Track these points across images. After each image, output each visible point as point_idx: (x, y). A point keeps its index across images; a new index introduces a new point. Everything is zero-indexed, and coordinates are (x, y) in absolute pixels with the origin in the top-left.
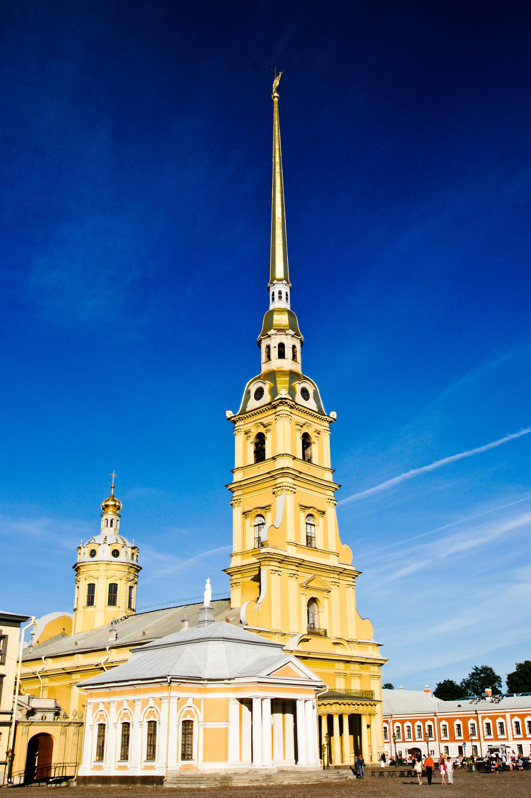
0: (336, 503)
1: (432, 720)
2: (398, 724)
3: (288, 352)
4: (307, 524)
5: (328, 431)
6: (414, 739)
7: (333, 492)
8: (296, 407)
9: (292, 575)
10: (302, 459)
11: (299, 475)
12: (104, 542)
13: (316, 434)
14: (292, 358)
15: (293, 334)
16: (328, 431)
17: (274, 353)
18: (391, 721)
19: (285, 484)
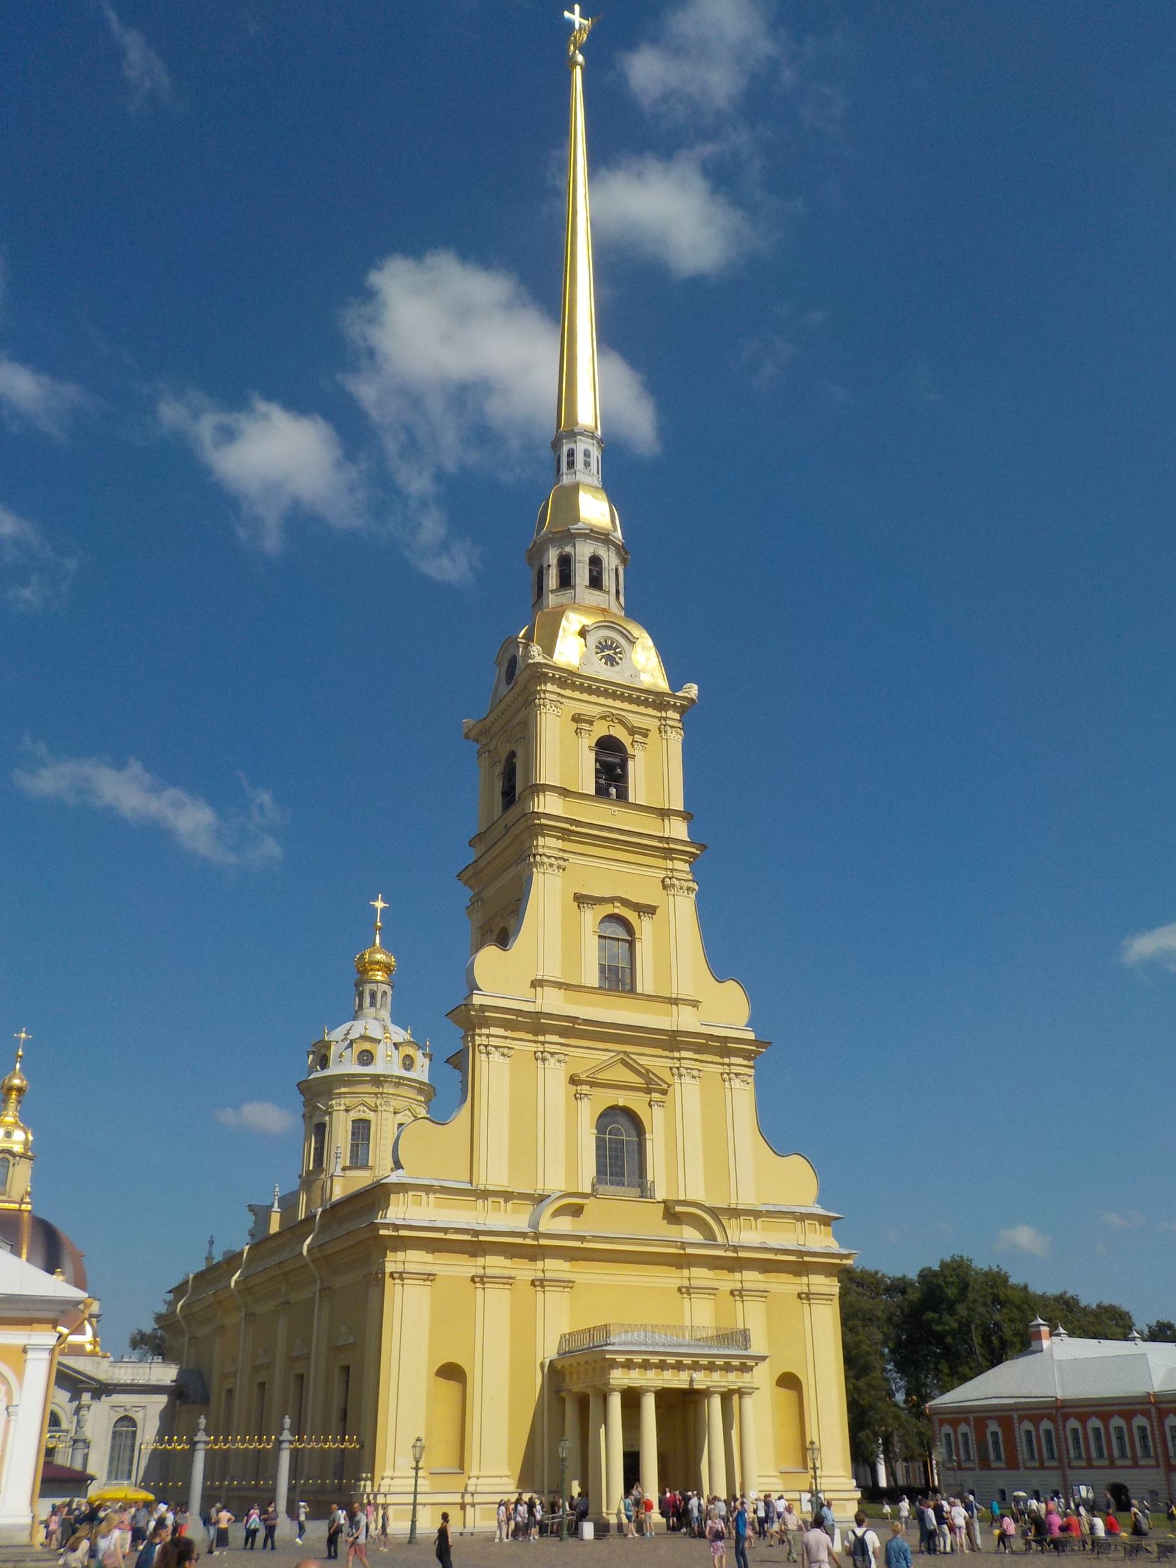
0: (696, 886)
1: (1146, 1414)
2: (1073, 1423)
3: (582, 575)
4: (600, 937)
6: (1134, 1459)
7: (685, 861)
8: (573, 683)
9: (546, 1054)
10: (594, 794)
11: (573, 828)
12: (344, 1037)
13: (638, 737)
14: (588, 584)
15: (588, 531)
17: (552, 580)
18: (1059, 1414)
19: (534, 852)
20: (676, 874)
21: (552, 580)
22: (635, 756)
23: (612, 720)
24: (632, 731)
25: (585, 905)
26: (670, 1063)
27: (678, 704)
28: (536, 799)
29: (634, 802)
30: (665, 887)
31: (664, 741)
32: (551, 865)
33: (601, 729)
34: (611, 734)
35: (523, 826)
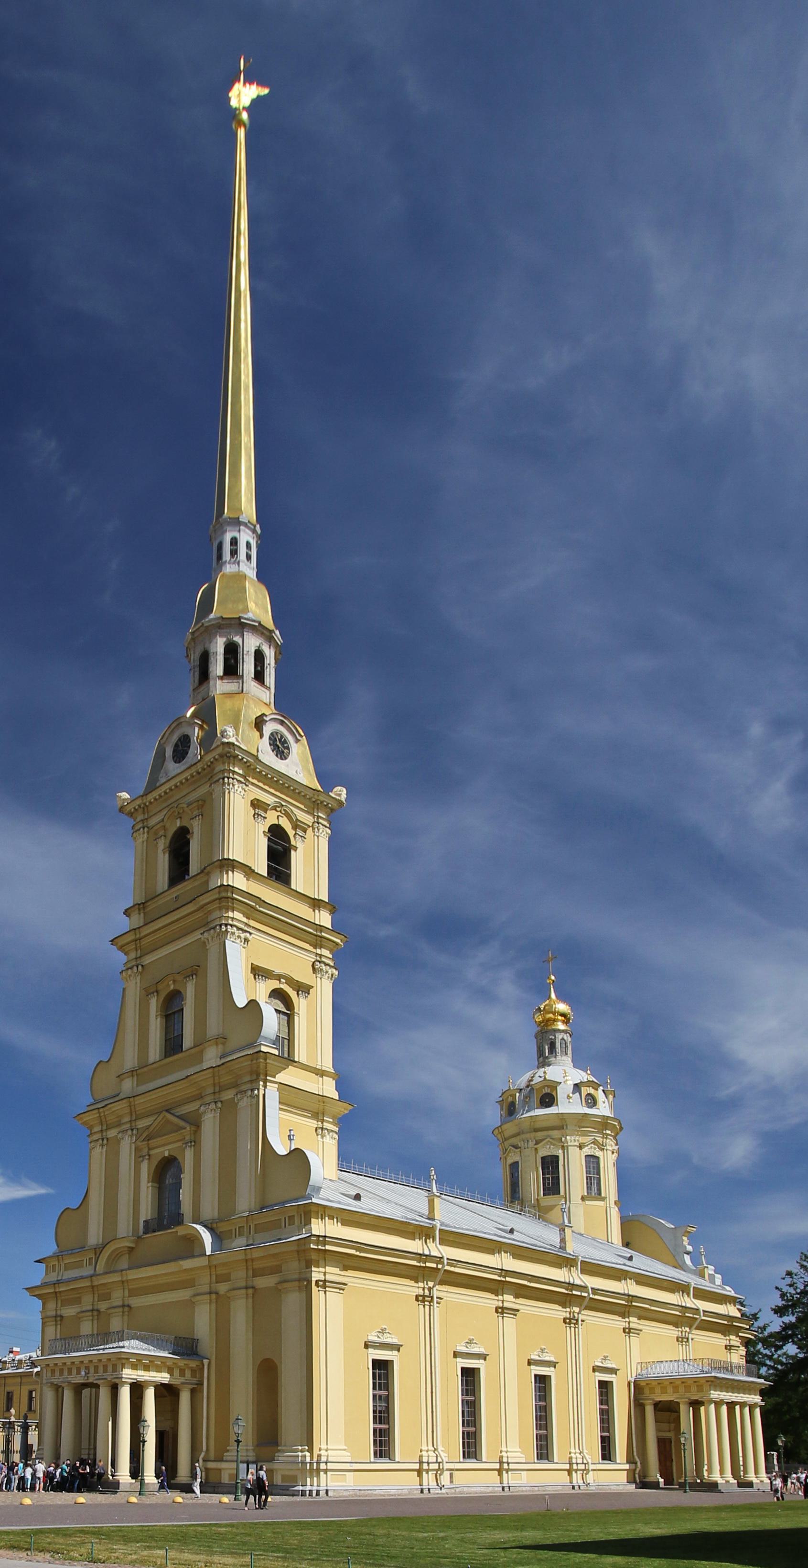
0: (336, 973)
5: (326, 827)
16: (326, 827)
17: (218, 667)
20: (323, 959)
21: (218, 667)
22: (297, 848)
23: (280, 811)
24: (296, 825)
25: (260, 977)
26: (314, 1124)
27: (330, 805)
28: (225, 876)
29: (295, 888)
30: (314, 970)
31: (316, 837)
32: (239, 937)
33: (272, 818)
34: (280, 823)
35: (217, 896)
